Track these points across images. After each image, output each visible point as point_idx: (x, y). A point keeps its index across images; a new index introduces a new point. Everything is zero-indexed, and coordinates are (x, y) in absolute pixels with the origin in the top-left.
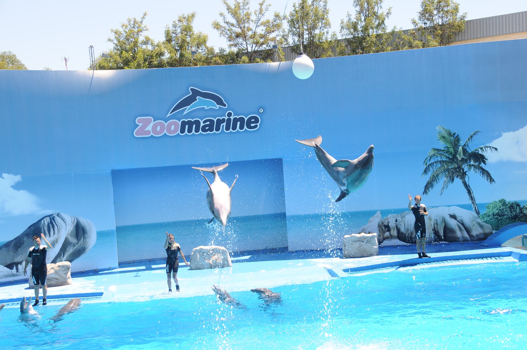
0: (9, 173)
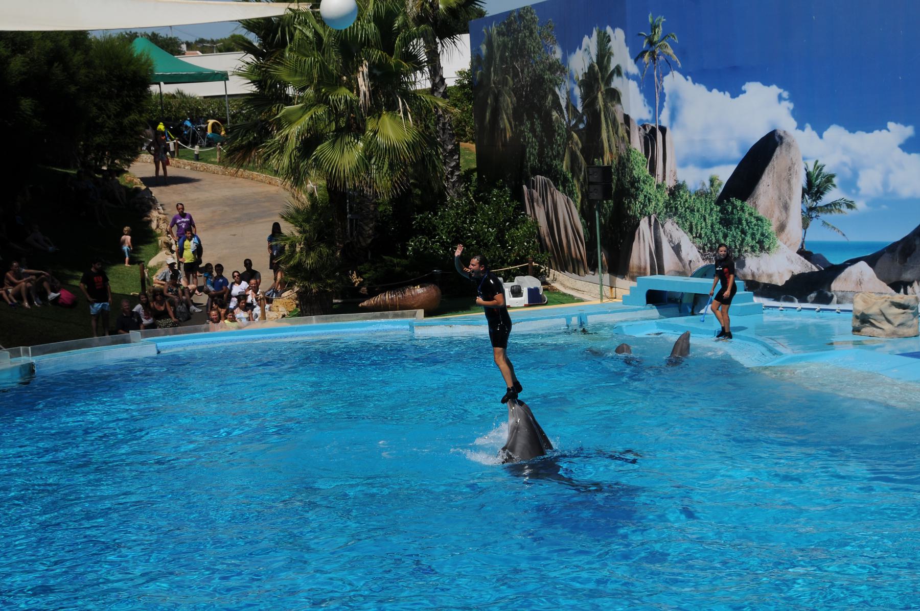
0: (896, 122)
